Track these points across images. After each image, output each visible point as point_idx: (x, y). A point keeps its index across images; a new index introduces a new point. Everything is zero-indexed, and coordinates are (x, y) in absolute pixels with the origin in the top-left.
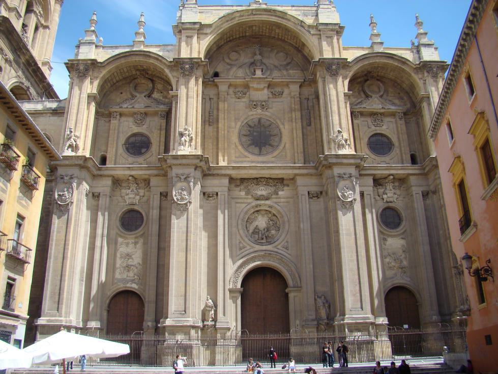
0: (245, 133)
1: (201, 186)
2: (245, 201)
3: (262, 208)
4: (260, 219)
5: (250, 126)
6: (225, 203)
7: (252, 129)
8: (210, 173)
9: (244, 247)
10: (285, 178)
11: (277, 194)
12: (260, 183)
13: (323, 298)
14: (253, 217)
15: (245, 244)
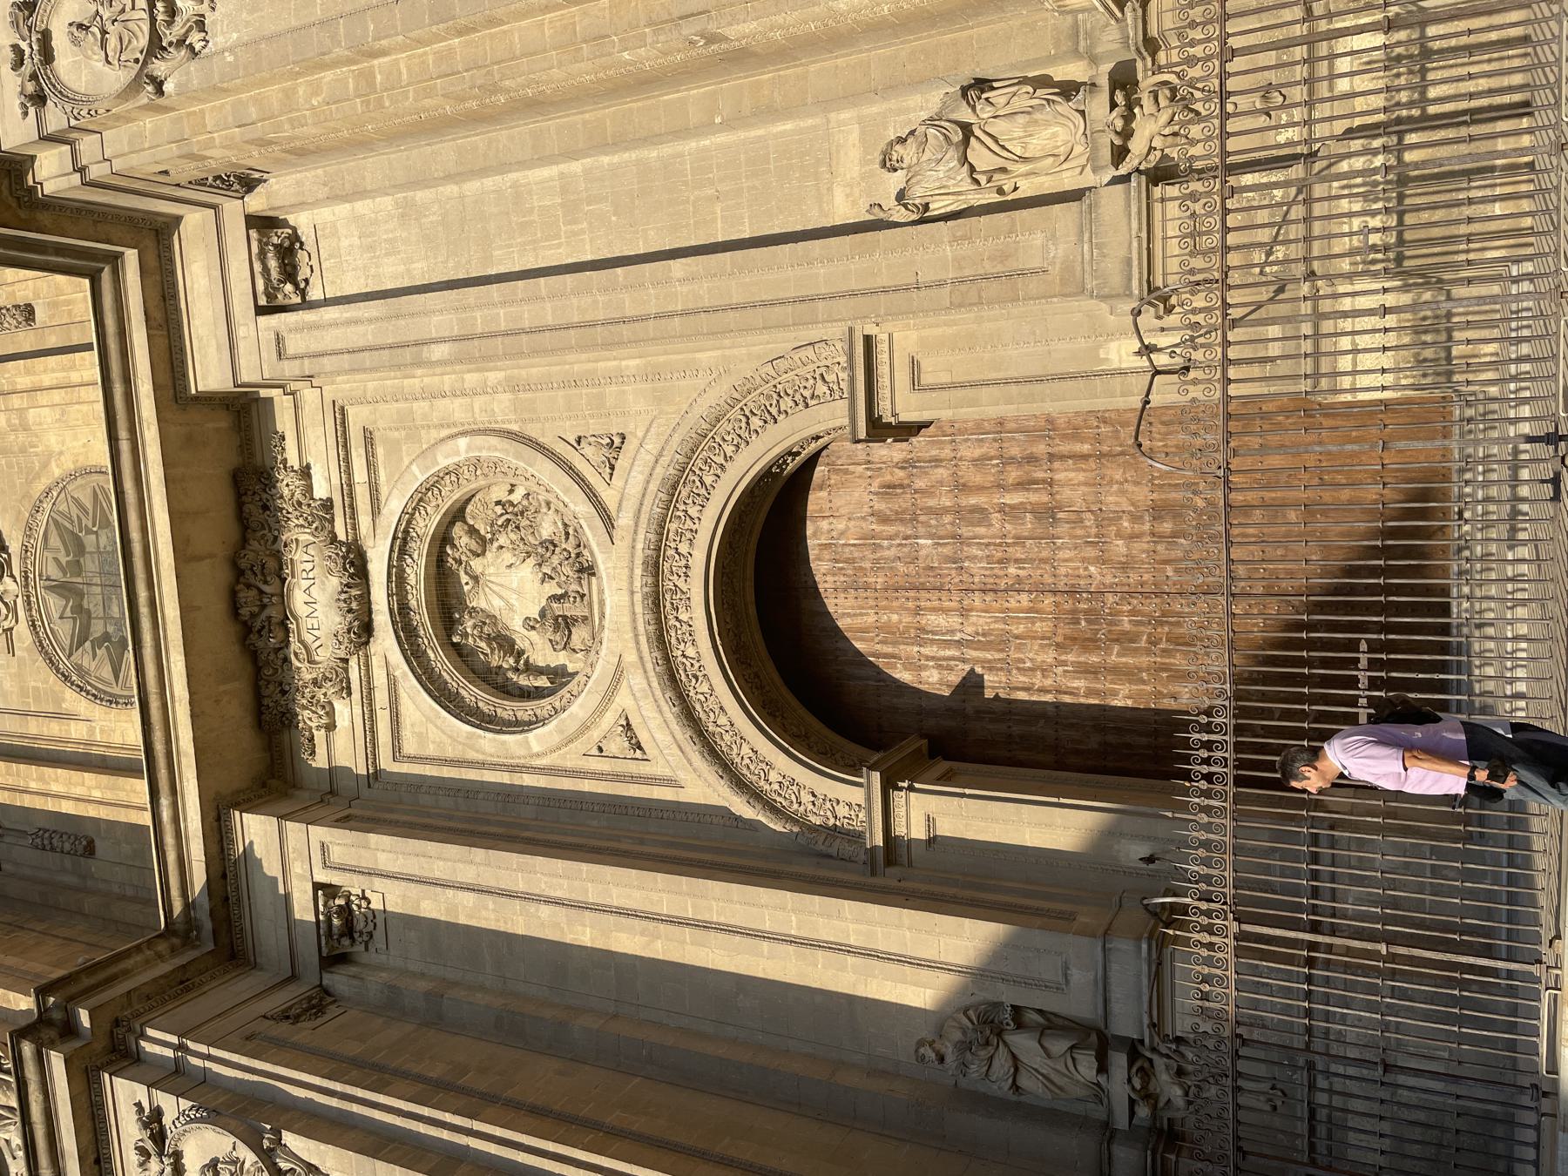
0: (107, 672)
1: (293, 977)
2: (381, 697)
3: (418, 596)
4: (497, 602)
5: (81, 639)
6: (367, 847)
7: (97, 629)
8: (208, 925)
9: (628, 727)
10: (233, 460)
11: (328, 505)
12: (273, 612)
13: (908, 153)
14: (483, 645)
15: (609, 718)
